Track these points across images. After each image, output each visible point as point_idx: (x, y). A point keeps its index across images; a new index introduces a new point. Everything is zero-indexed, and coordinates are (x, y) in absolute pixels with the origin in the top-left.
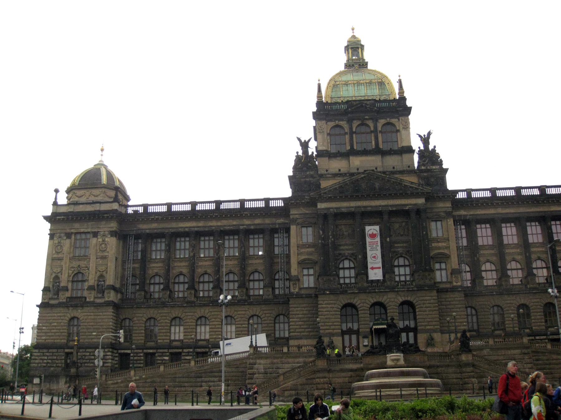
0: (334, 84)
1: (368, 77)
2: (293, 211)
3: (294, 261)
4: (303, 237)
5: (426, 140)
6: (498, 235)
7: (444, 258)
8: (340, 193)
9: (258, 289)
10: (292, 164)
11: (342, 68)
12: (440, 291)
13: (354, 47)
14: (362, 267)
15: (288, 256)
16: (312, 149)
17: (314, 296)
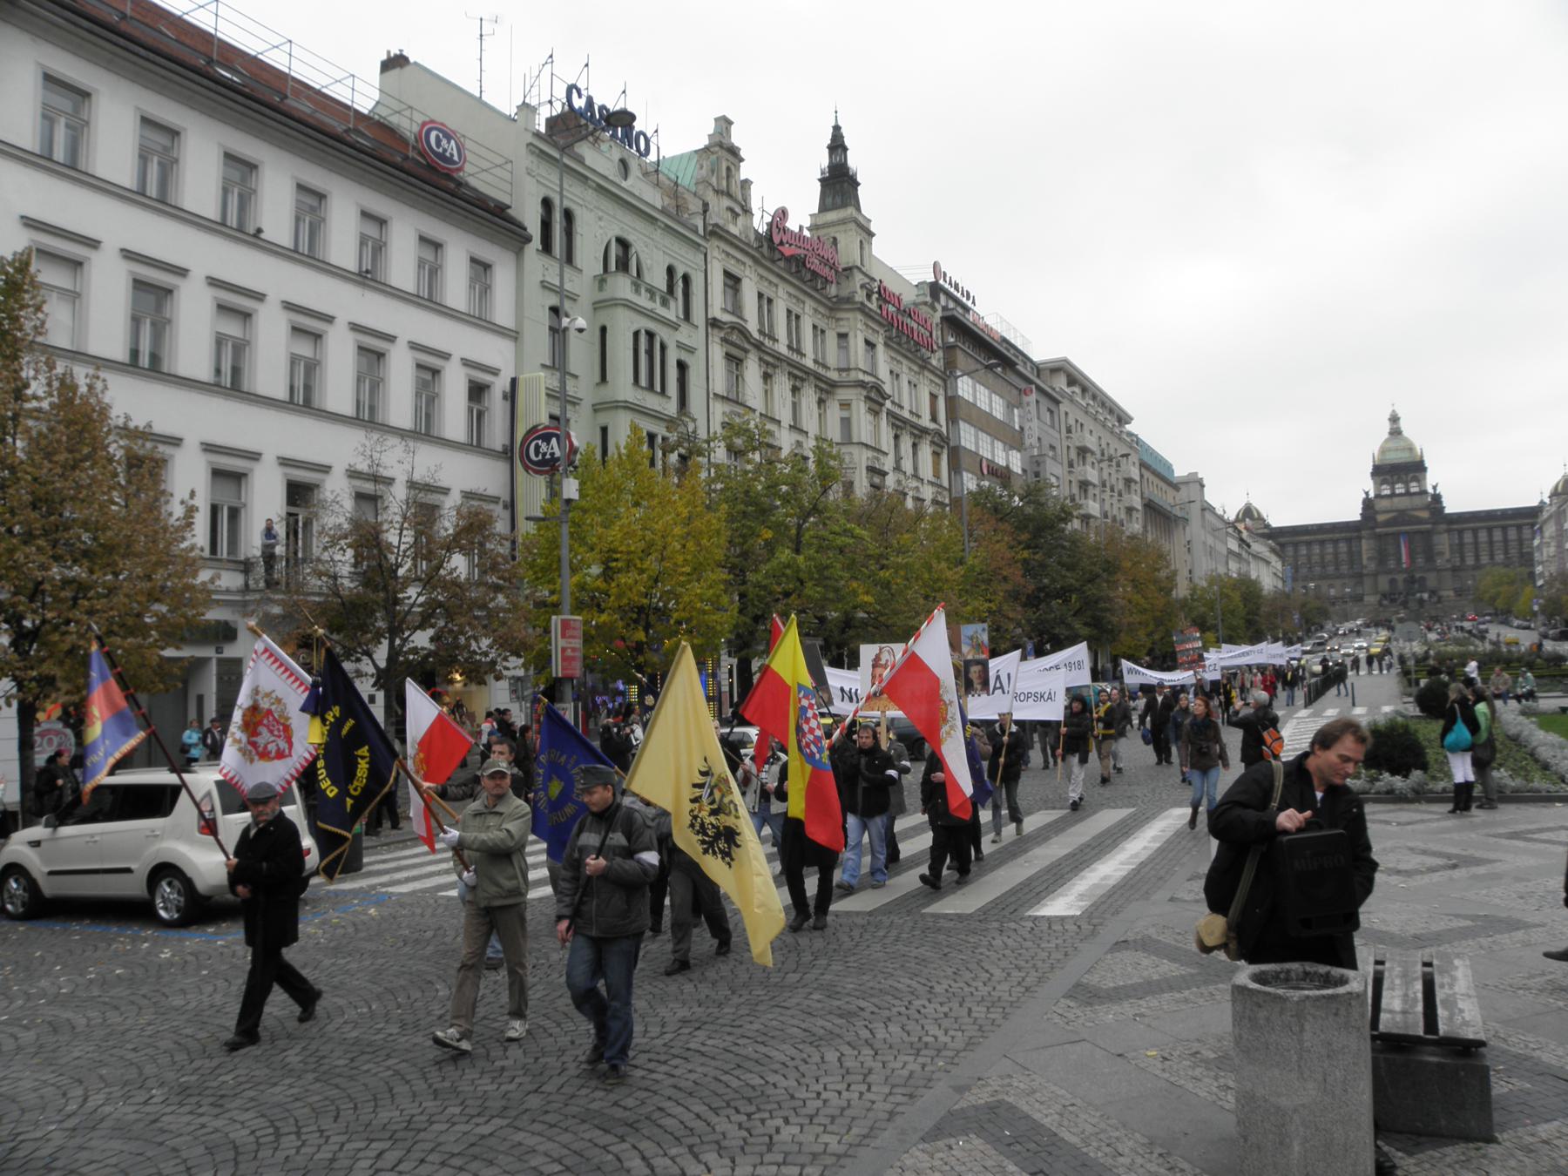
0: (1383, 451)
1: (1402, 444)
2: (1364, 533)
3: (1365, 557)
4: (1366, 547)
5: (1435, 488)
6: (1476, 537)
7: (1441, 554)
8: (1387, 523)
9: (1344, 569)
10: (1361, 506)
11: (1386, 436)
12: (1439, 571)
13: (1394, 419)
14: (1399, 560)
15: (1360, 553)
16: (1372, 495)
17: (1375, 575)
